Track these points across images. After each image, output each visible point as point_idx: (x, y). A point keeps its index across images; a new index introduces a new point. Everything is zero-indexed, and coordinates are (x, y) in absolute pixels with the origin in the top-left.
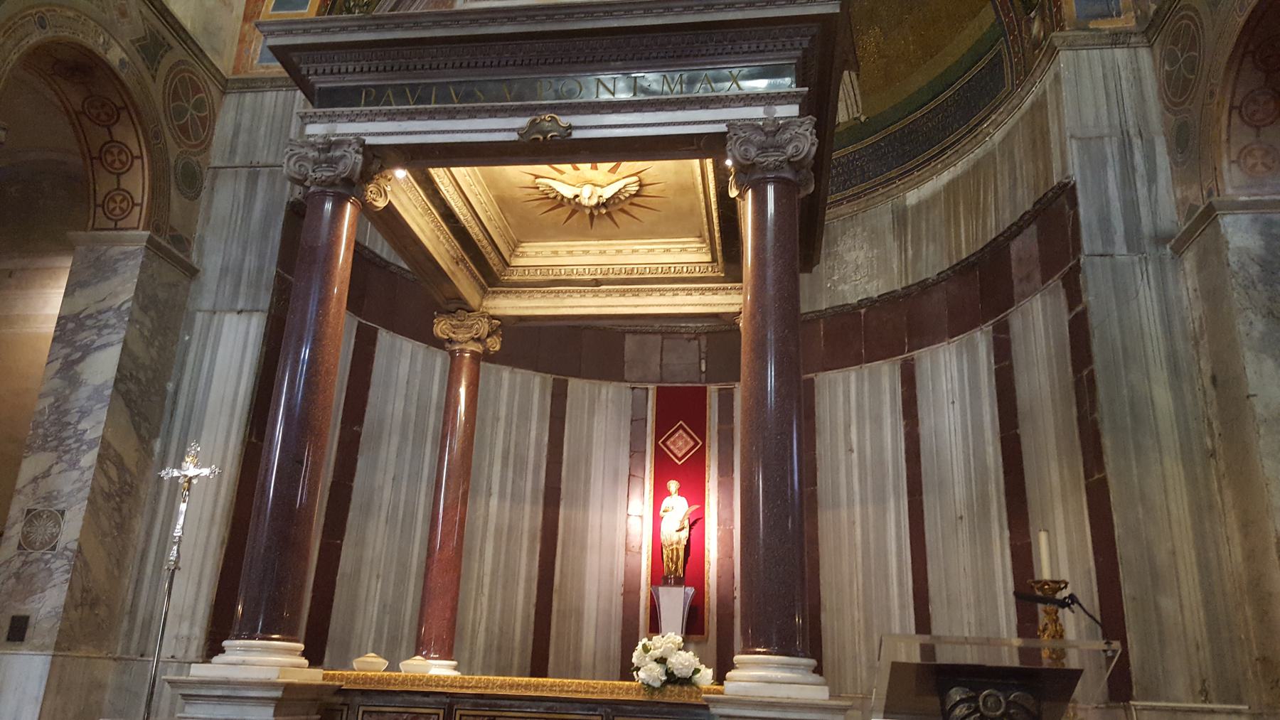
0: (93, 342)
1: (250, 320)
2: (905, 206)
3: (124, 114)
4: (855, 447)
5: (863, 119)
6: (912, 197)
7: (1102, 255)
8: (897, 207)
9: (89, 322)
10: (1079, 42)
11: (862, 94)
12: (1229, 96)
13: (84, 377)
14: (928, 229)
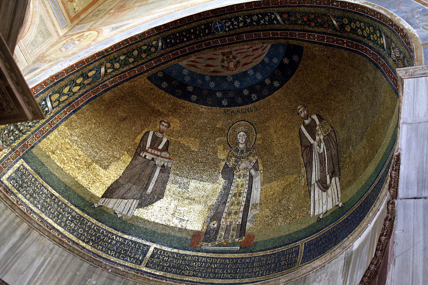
2: (352, 252)
5: (340, 205)
6: (356, 245)
7: (415, 198)
8: (348, 254)
10: (418, 72)
11: (341, 189)
14: (359, 262)
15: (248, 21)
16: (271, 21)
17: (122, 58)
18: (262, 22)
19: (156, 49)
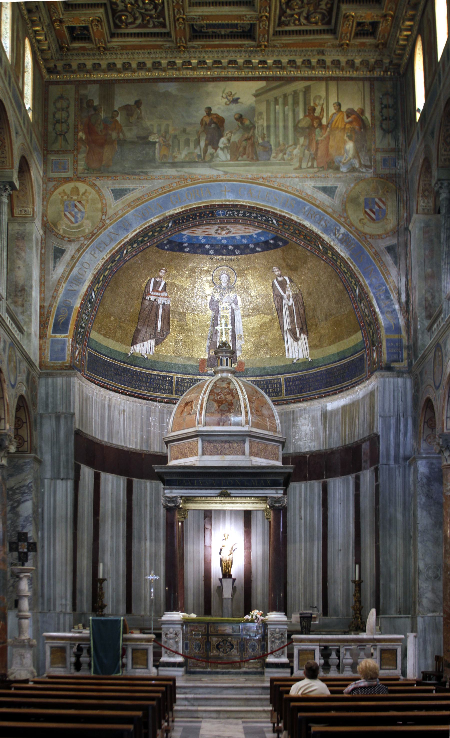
0: (21, 499)
1: (67, 483)
3: (22, 408)
4: (303, 518)
9: (18, 491)
12: (423, 418)
13: (21, 513)
15: (247, 214)
16: (267, 220)
17: (140, 239)
18: (260, 219)
19: (167, 228)
